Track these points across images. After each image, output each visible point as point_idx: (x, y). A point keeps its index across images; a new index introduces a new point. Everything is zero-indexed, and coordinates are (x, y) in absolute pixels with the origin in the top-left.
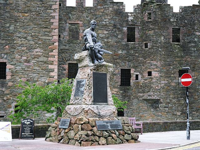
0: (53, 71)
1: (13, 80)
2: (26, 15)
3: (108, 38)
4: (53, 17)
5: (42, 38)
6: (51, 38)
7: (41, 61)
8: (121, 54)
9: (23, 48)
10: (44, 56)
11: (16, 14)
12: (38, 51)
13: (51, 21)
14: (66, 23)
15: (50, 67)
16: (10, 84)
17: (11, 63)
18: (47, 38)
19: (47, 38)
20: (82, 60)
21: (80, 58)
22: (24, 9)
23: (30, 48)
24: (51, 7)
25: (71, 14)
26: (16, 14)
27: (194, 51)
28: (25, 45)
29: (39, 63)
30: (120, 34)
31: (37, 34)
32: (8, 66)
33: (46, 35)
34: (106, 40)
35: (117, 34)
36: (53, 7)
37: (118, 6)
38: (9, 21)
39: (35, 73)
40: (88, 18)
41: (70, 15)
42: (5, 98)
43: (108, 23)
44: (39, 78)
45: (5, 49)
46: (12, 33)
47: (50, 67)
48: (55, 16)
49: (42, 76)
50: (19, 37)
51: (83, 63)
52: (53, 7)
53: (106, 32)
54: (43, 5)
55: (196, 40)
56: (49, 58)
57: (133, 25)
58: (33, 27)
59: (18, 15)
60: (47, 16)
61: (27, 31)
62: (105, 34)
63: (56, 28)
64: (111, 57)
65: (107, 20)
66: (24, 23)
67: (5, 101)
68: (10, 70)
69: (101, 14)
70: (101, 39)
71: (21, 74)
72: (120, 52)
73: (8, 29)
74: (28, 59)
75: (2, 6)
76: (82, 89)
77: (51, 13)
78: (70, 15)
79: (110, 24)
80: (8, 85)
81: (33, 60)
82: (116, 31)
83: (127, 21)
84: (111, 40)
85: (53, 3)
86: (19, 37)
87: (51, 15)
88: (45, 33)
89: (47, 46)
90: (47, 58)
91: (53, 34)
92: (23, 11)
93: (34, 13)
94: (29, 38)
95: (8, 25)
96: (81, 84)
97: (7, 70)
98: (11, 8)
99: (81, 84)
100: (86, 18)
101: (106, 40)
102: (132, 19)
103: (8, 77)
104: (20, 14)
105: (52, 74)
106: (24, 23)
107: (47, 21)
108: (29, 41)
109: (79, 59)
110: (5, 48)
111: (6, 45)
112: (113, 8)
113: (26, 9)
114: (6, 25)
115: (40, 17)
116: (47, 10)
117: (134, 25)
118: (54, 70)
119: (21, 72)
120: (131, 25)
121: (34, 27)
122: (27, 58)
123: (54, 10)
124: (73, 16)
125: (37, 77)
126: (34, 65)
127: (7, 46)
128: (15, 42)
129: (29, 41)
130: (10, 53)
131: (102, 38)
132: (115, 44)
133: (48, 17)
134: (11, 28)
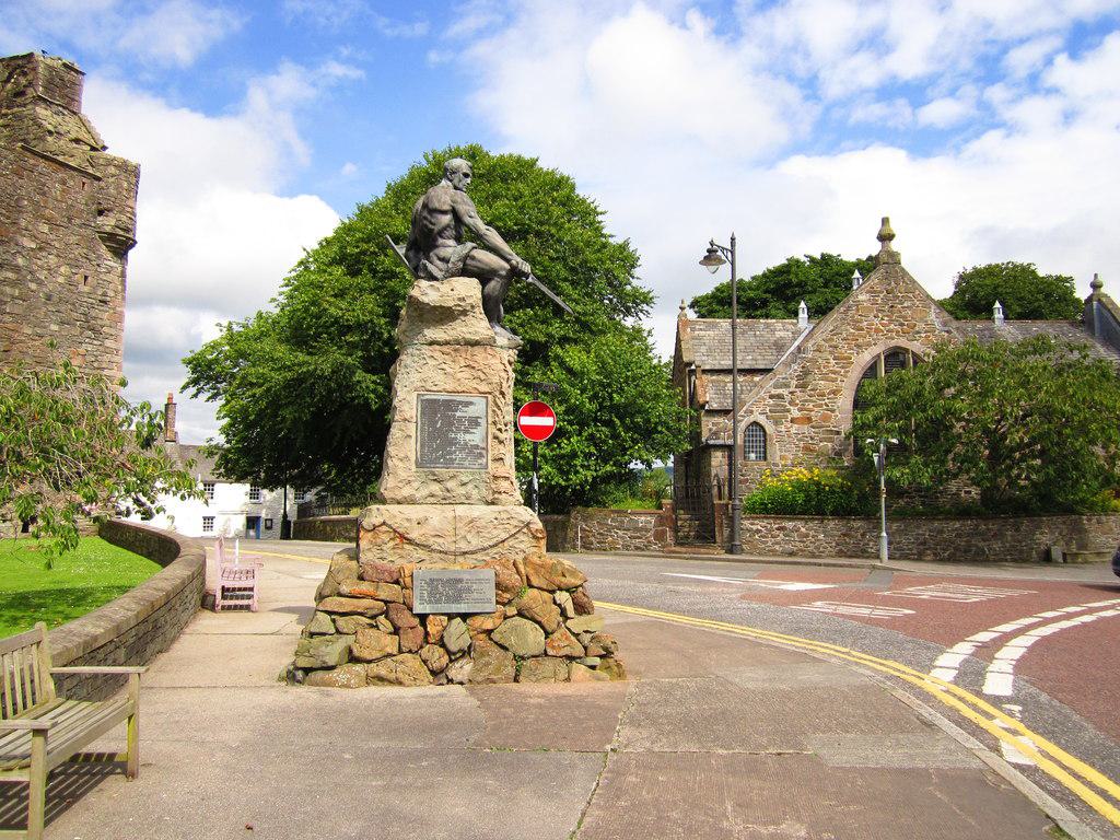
20: (464, 313)
27: (13, 297)
51: (464, 329)
55: (20, 261)
76: (468, 437)
96: (458, 414)
99: (458, 414)
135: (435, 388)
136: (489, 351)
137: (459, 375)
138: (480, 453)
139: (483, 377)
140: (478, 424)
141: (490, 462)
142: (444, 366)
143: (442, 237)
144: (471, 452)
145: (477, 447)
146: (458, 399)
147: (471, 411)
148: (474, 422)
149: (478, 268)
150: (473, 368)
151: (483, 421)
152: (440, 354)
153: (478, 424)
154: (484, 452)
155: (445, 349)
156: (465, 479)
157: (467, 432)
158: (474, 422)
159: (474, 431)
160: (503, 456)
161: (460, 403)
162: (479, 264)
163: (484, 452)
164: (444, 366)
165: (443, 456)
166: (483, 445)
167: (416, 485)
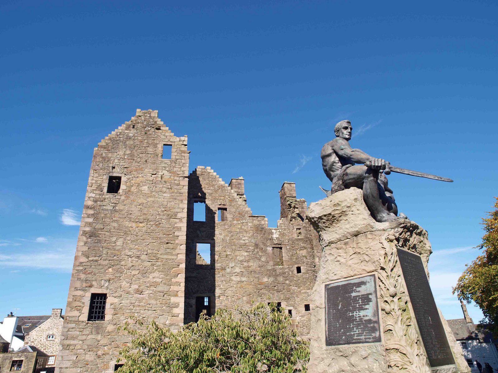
0: (177, 306)
1: (114, 322)
2: (141, 225)
3: (248, 261)
4: (179, 229)
5: (162, 257)
6: (174, 257)
7: (159, 292)
8: (267, 281)
9: (133, 272)
10: (165, 284)
11: (127, 224)
12: (156, 276)
13: (175, 234)
14: (193, 243)
15: (173, 300)
16: (110, 328)
17: (114, 295)
18: (170, 257)
19: (170, 257)
20: (343, 213)
21: (335, 210)
22: (139, 217)
23: (144, 273)
24: (176, 215)
25: (199, 230)
26: (127, 224)
28: (137, 268)
29: (158, 295)
30: (264, 255)
31: (155, 252)
32: (109, 300)
33: (167, 254)
34: (245, 264)
35: (259, 255)
36: (179, 215)
37: (258, 221)
38: (116, 233)
39: (150, 309)
40: (221, 236)
41: (198, 232)
42: (100, 353)
43: (247, 241)
44: (156, 317)
45: (107, 273)
46: (118, 250)
47: (173, 300)
48: (181, 227)
49: (161, 314)
50: (130, 256)
51: (348, 226)
52: (179, 215)
53: (246, 254)
54: (165, 212)
56: (172, 287)
57: (279, 244)
58: (150, 243)
59: (130, 225)
60: (170, 227)
61: (140, 248)
62: (245, 257)
63: (182, 244)
64: (254, 287)
65: (246, 238)
66: (137, 236)
67: (99, 357)
68: (112, 306)
69: (238, 230)
70: (239, 262)
71: (128, 311)
72: (265, 280)
73: (114, 245)
74: (141, 287)
75: (108, 213)
76: (362, 313)
77: (176, 223)
78: (198, 232)
79: (251, 244)
80: (107, 331)
81: (147, 289)
82: (258, 252)
83: (272, 239)
84: (252, 265)
85: (179, 210)
86: (130, 256)
87: (176, 225)
88: (166, 250)
89: (169, 268)
90: (168, 287)
91: (177, 251)
92: (137, 220)
93: (152, 223)
94: (143, 257)
95: (114, 239)
96: (354, 294)
97: (108, 306)
98: (121, 216)
99: (354, 294)
100: (220, 236)
101: (245, 264)
102: (278, 236)
103: (108, 316)
104: (134, 225)
105: (175, 311)
106: (137, 236)
107: (170, 233)
108: (143, 261)
109: (330, 214)
110: (107, 271)
111: (109, 268)
112: (252, 223)
113: (141, 217)
114: (111, 238)
115: (161, 229)
116: (171, 219)
117: (281, 244)
118: (179, 304)
119: (129, 308)
120: (277, 244)
121: (151, 241)
122: (140, 286)
123: (181, 220)
124: (202, 234)
125: (153, 315)
126: (150, 297)
127: (110, 270)
128: (123, 263)
129: (143, 261)
130: (113, 279)
131: (242, 261)
132: (259, 269)
133: (171, 229)
134: (118, 243)
135: (335, 278)
136: (369, 236)
137: (350, 262)
138: (374, 327)
139: (367, 258)
140: (369, 300)
141: (382, 334)
142: (339, 258)
143: (333, 171)
144: (366, 326)
145: (370, 321)
146: (352, 282)
147: (363, 290)
148: (366, 299)
149: (352, 179)
150: (359, 253)
151: (372, 297)
152: (335, 250)
153: (369, 300)
154: (376, 325)
155: (339, 245)
156: (364, 354)
157: (361, 309)
158: (366, 299)
159: (367, 307)
160: (391, 327)
161: (354, 284)
162: (351, 177)
163: (376, 325)
164: (339, 258)
165: (344, 333)
166: (374, 319)
167: (327, 361)
